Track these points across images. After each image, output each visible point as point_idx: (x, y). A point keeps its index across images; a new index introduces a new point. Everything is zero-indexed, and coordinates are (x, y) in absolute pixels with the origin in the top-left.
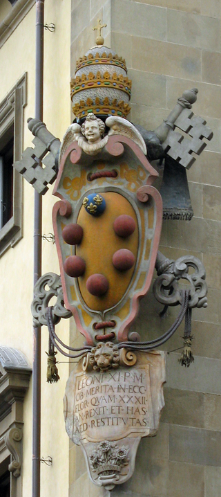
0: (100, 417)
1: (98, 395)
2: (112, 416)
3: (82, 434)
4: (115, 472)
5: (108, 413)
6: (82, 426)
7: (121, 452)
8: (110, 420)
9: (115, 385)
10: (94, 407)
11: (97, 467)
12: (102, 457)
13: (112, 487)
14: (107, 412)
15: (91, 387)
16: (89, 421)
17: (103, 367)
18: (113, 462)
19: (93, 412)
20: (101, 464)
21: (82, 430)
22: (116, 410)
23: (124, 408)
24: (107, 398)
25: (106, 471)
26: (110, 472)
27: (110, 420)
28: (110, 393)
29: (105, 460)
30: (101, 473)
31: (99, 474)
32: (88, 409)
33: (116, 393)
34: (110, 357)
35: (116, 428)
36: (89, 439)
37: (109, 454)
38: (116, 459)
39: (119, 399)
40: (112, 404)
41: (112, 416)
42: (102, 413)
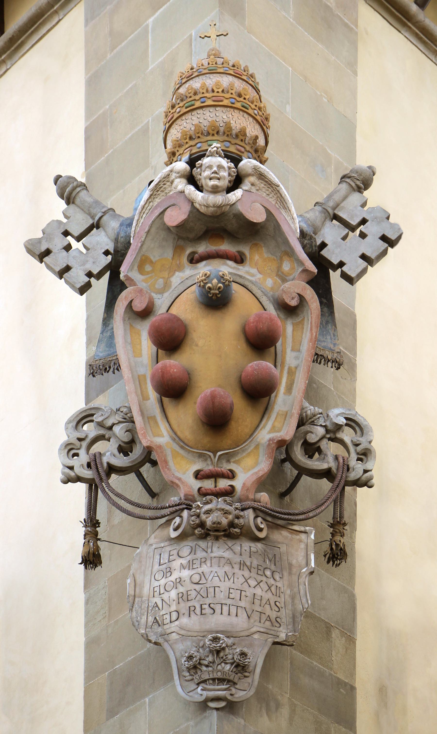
0: (208, 601)
1: (205, 568)
2: (229, 602)
3: (165, 627)
4: (229, 681)
5: (222, 595)
6: (168, 616)
7: (243, 654)
8: (225, 608)
9: (237, 559)
10: (198, 587)
11: (196, 673)
12: (210, 658)
13: (222, 704)
14: (221, 596)
15: (189, 558)
16: (184, 607)
17: (217, 531)
18: (228, 667)
19: (193, 594)
20: (204, 668)
21: (168, 621)
22: (235, 594)
23: (248, 594)
24: (221, 574)
25: (214, 680)
26: (221, 681)
27: (225, 608)
28: (227, 568)
29: (214, 662)
30: (204, 681)
31: (198, 684)
32: (181, 589)
33: (236, 570)
34: (230, 517)
35: (234, 620)
36: (182, 632)
37: (222, 654)
38: (232, 664)
39: (242, 580)
40: (228, 584)
41: (229, 602)
42: (211, 594)
